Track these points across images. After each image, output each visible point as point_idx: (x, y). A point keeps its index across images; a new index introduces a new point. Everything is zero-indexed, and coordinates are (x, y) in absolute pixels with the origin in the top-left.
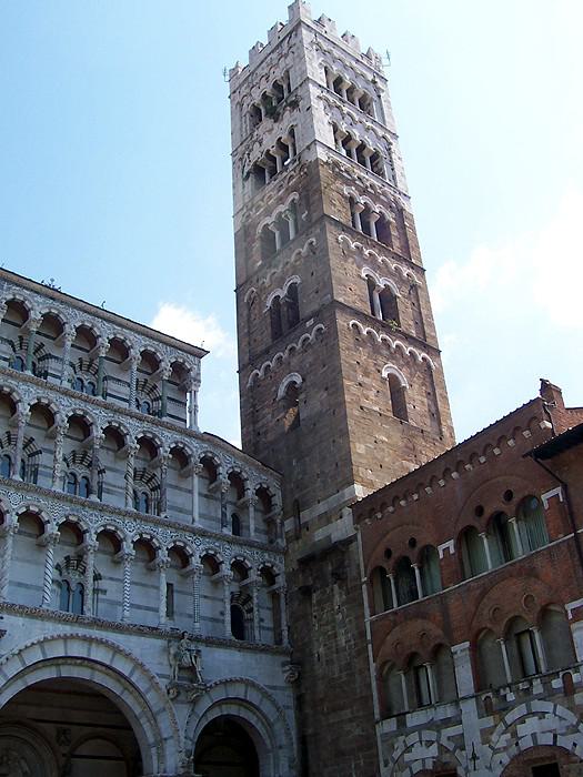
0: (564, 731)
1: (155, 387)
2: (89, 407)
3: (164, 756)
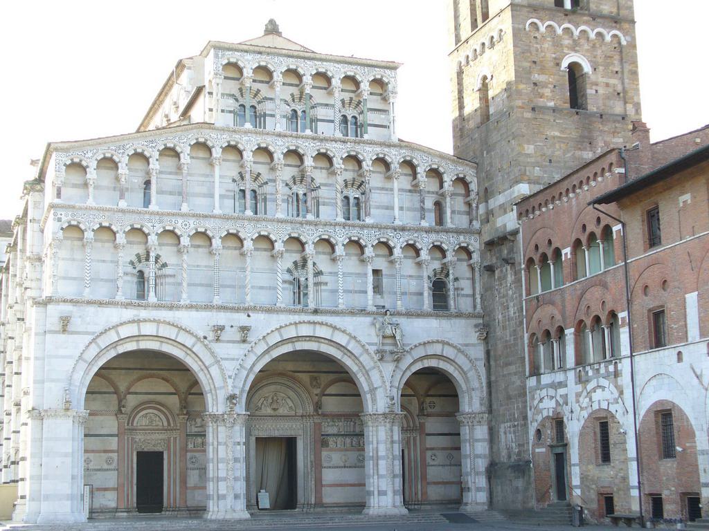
0: (612, 401)
1: (359, 102)
2: (300, 142)
3: (375, 400)
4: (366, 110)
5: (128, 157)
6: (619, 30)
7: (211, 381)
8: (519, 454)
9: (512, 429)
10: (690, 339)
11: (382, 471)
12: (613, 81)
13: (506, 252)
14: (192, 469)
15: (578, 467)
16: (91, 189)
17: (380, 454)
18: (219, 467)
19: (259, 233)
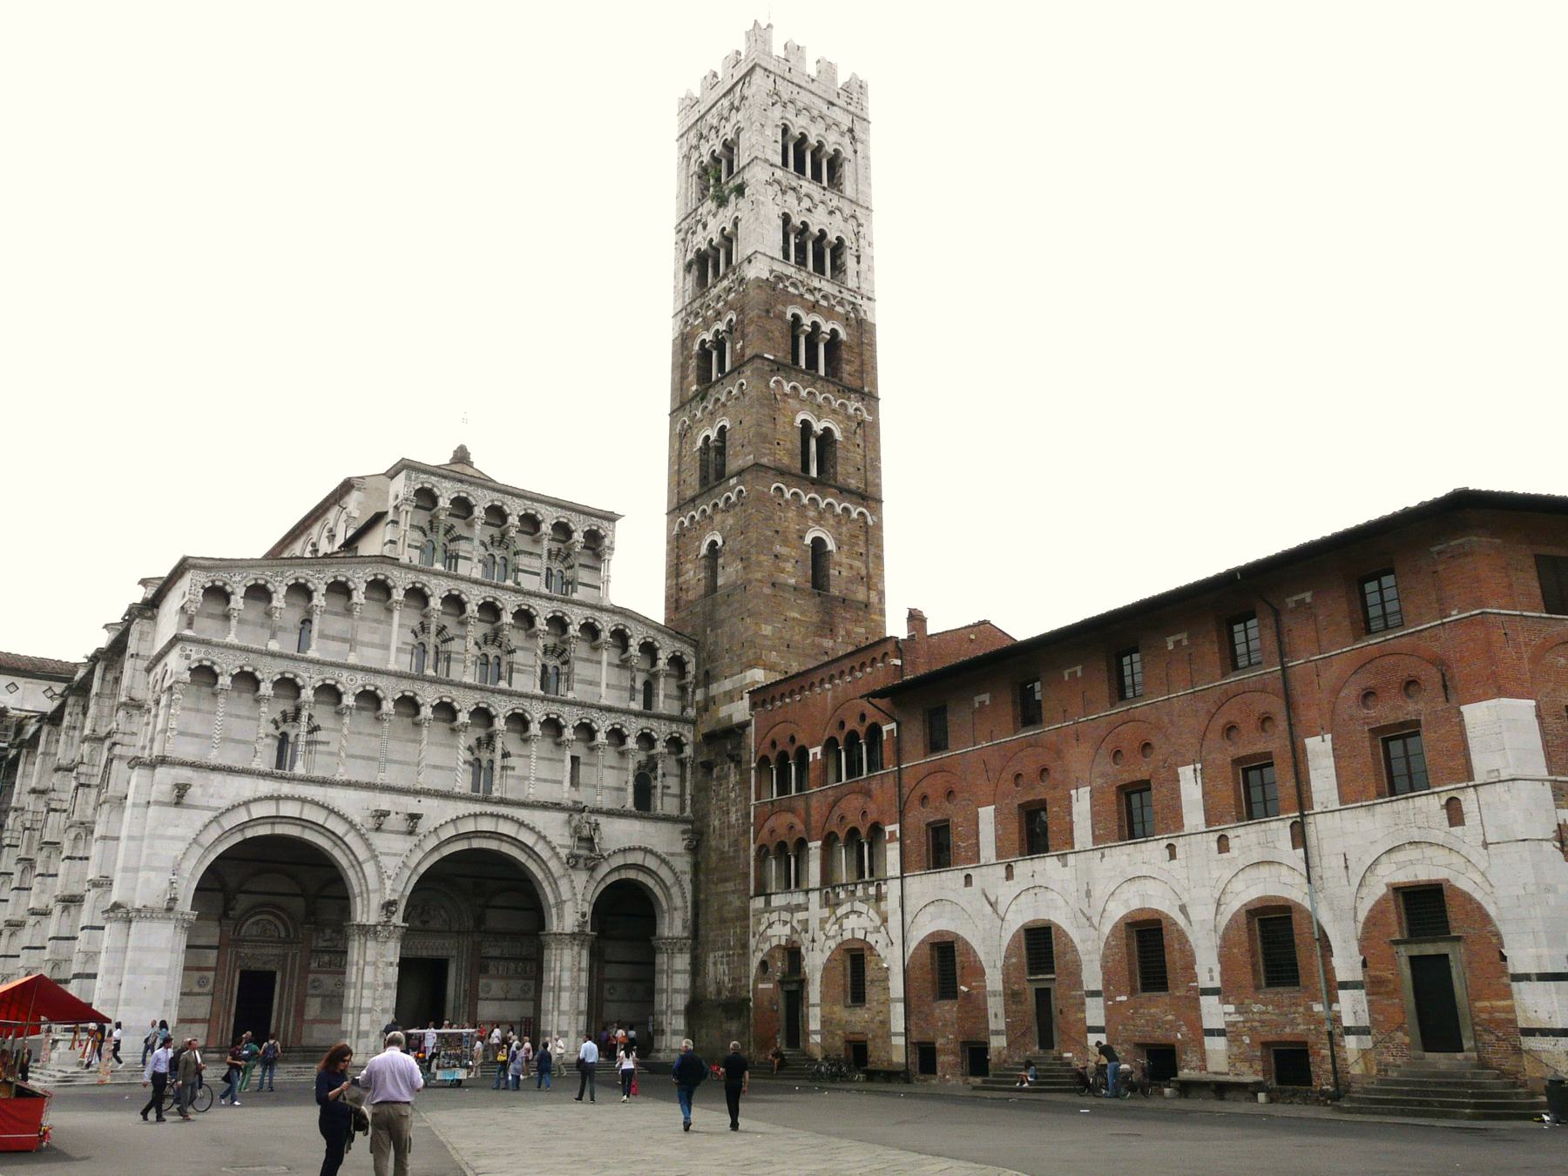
1: (568, 555)
2: (499, 594)
3: (563, 916)
4: (577, 565)
5: (286, 588)
6: (866, 508)
7: (363, 881)
8: (733, 989)
9: (725, 960)
10: (982, 861)
11: (565, 1006)
12: (857, 564)
13: (729, 747)
14: (312, 996)
15: (818, 1009)
16: (234, 622)
17: (563, 984)
18: (364, 995)
19: (441, 698)
